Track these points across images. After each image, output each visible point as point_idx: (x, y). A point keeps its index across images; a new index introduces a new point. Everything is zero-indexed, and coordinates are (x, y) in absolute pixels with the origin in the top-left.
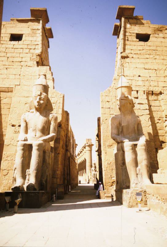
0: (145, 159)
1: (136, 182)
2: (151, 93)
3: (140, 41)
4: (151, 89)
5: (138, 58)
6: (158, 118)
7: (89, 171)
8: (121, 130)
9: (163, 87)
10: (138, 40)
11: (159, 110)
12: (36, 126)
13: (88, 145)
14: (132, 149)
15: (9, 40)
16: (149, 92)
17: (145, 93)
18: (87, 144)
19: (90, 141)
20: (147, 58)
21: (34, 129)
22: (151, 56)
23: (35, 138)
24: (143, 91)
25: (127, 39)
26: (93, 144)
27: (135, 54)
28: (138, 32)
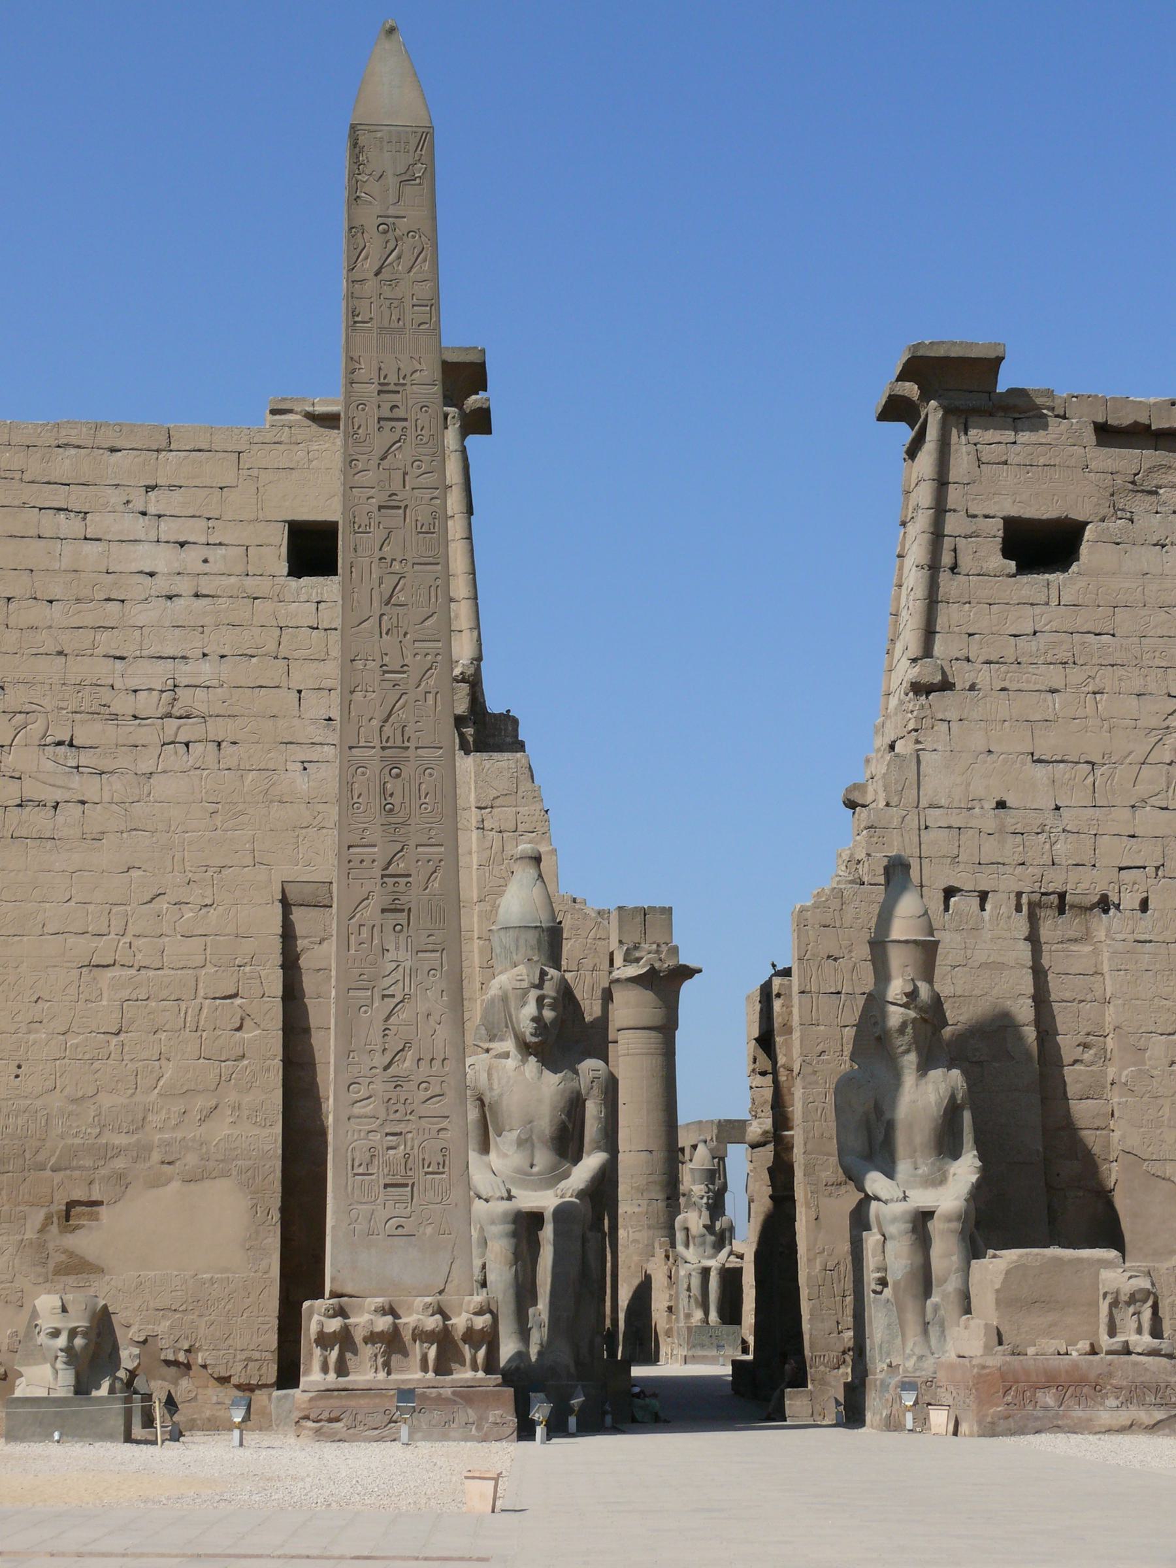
0: (957, 1271)
1: (918, 1351)
2: (1056, 902)
3: (1022, 569)
4: (1055, 881)
5: (1003, 689)
6: (1081, 1038)
7: (643, 1236)
8: (881, 1137)
9: (1121, 869)
10: (1012, 565)
11: (1089, 997)
12: (530, 1122)
13: (632, 971)
14: (914, 1230)
15: (285, 571)
16: (1044, 898)
17: (1025, 908)
18: (629, 959)
19: (655, 934)
20: (1054, 691)
21: (523, 1137)
22: (1076, 675)
23: (531, 1175)
24: (1013, 896)
25: (946, 559)
26: (685, 959)
27: (989, 662)
28: (1014, 511)
